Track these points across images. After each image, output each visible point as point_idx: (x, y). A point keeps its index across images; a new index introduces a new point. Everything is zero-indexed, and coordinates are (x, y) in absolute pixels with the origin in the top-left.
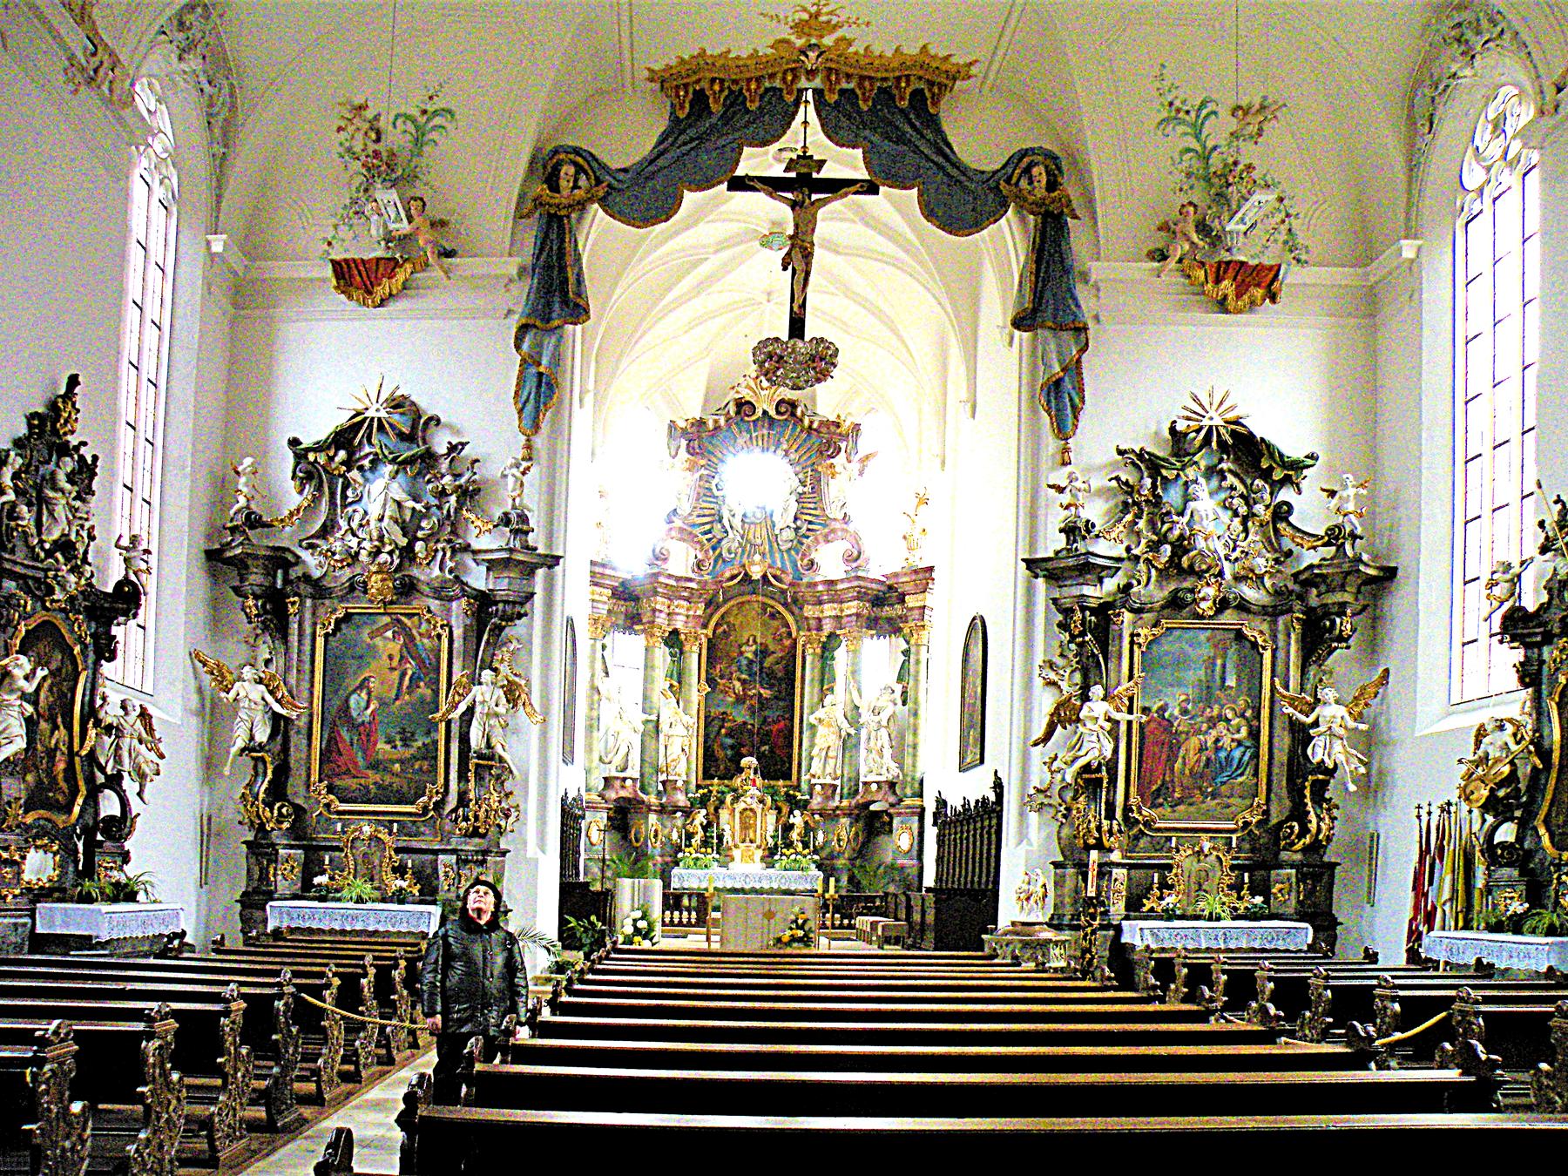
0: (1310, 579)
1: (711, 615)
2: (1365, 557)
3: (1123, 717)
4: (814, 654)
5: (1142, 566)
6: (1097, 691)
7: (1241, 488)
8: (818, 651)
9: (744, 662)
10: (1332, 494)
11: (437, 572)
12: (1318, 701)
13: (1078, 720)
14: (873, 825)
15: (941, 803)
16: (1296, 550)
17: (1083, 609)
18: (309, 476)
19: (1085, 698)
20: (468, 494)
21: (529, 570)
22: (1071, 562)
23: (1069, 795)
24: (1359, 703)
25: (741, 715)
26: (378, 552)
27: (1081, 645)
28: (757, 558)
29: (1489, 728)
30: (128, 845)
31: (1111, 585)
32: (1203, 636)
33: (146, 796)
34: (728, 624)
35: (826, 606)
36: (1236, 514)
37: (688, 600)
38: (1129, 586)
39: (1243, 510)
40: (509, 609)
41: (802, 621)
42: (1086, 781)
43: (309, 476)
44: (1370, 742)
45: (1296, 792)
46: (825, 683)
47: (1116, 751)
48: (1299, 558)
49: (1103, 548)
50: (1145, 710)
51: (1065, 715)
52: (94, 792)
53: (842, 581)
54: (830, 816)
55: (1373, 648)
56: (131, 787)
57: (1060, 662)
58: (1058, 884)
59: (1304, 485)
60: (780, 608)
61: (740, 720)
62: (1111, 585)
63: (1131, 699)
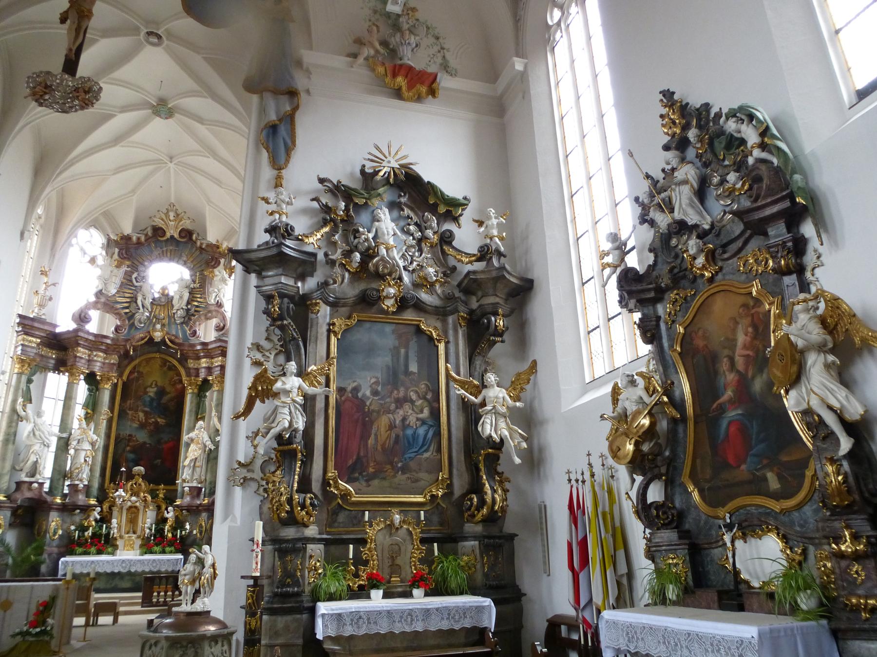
1: (127, 366)
4: (193, 393)
8: (196, 391)
9: (148, 399)
25: (142, 437)
28: (158, 326)
34: (138, 372)
35: (204, 360)
37: (105, 352)
41: (188, 370)
46: (199, 414)
53: (211, 342)
60: (176, 363)
61: (141, 440)
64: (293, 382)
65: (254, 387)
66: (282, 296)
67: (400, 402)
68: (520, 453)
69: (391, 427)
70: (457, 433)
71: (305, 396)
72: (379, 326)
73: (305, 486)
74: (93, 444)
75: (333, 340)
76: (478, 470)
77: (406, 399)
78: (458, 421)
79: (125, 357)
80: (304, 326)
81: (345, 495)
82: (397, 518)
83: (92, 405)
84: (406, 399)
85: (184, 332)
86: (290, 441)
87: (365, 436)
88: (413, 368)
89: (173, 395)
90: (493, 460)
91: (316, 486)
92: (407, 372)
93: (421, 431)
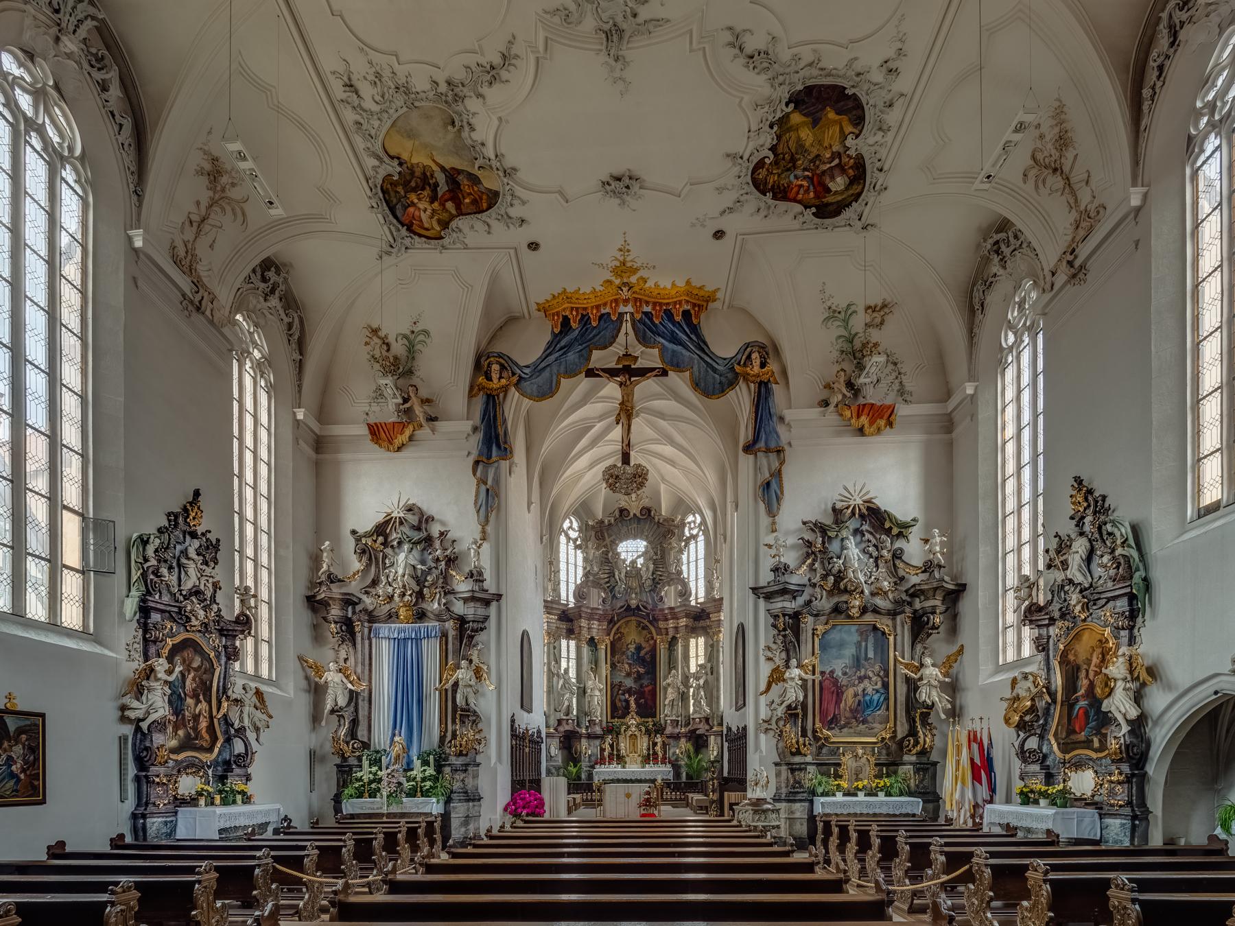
0: (915, 593)
2: (946, 578)
3: (809, 677)
5: (818, 590)
6: (794, 662)
7: (874, 541)
10: (926, 541)
11: (436, 605)
12: (922, 665)
13: (784, 680)
14: (699, 742)
15: (729, 729)
16: (907, 576)
17: (784, 615)
18: (364, 552)
19: (788, 667)
20: (451, 561)
21: (487, 603)
22: (776, 588)
23: (782, 723)
24: (948, 664)
25: (629, 683)
26: (404, 595)
27: (784, 636)
29: (1019, 678)
30: (249, 770)
31: (801, 600)
32: (854, 629)
33: (261, 739)
36: (871, 556)
38: (810, 601)
39: (875, 554)
40: (475, 625)
42: (791, 715)
43: (364, 552)
44: (952, 688)
45: (911, 721)
46: (672, 665)
47: (806, 696)
48: (908, 580)
49: (794, 580)
50: (822, 673)
51: (776, 677)
52: (228, 740)
54: (676, 737)
55: (953, 631)
56: (251, 736)
57: (774, 647)
58: (778, 775)
59: (910, 537)
62: (801, 600)
63: (814, 667)
64: (795, 672)
65: (771, 675)
66: (784, 615)
67: (861, 679)
68: (946, 712)
69: (856, 695)
70: (901, 698)
71: (801, 679)
72: (846, 628)
73: (804, 734)
74: (600, 691)
75: (817, 640)
76: (915, 722)
77: (866, 677)
78: (902, 689)
79: (611, 622)
80: (797, 632)
81: (827, 739)
82: (860, 752)
83: (596, 662)
84: (866, 677)
85: (653, 599)
86: (796, 708)
87: (838, 702)
88: (871, 655)
89: (648, 649)
90: (924, 717)
91: (810, 734)
92: (867, 659)
93: (876, 697)
